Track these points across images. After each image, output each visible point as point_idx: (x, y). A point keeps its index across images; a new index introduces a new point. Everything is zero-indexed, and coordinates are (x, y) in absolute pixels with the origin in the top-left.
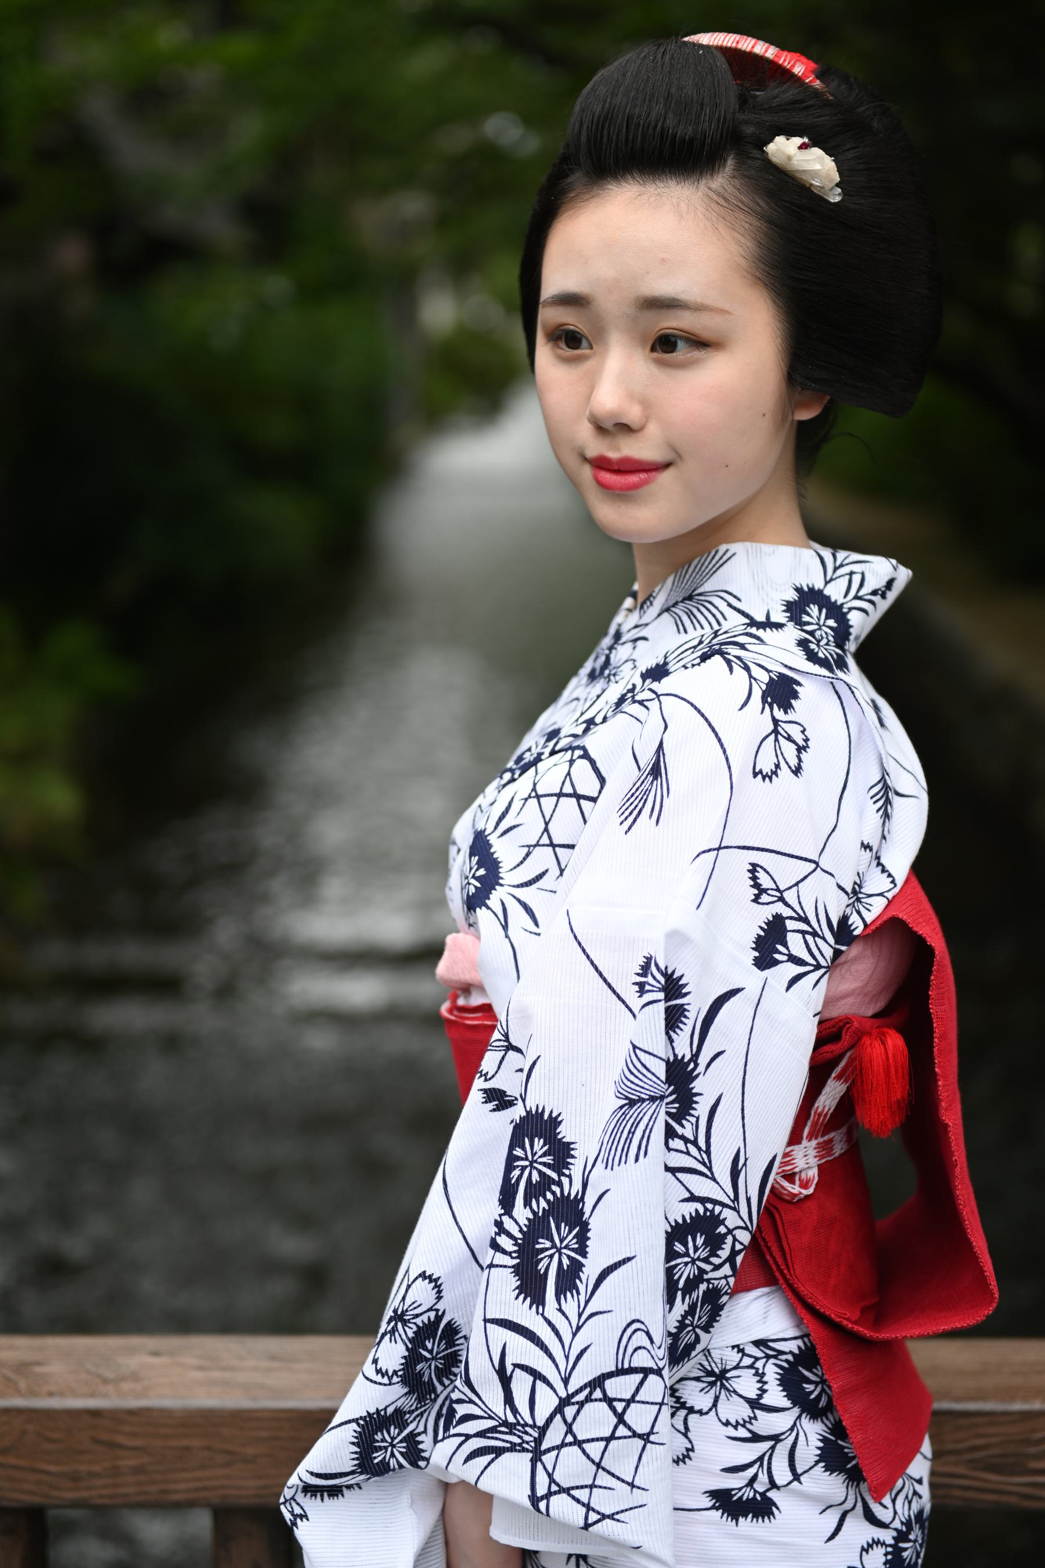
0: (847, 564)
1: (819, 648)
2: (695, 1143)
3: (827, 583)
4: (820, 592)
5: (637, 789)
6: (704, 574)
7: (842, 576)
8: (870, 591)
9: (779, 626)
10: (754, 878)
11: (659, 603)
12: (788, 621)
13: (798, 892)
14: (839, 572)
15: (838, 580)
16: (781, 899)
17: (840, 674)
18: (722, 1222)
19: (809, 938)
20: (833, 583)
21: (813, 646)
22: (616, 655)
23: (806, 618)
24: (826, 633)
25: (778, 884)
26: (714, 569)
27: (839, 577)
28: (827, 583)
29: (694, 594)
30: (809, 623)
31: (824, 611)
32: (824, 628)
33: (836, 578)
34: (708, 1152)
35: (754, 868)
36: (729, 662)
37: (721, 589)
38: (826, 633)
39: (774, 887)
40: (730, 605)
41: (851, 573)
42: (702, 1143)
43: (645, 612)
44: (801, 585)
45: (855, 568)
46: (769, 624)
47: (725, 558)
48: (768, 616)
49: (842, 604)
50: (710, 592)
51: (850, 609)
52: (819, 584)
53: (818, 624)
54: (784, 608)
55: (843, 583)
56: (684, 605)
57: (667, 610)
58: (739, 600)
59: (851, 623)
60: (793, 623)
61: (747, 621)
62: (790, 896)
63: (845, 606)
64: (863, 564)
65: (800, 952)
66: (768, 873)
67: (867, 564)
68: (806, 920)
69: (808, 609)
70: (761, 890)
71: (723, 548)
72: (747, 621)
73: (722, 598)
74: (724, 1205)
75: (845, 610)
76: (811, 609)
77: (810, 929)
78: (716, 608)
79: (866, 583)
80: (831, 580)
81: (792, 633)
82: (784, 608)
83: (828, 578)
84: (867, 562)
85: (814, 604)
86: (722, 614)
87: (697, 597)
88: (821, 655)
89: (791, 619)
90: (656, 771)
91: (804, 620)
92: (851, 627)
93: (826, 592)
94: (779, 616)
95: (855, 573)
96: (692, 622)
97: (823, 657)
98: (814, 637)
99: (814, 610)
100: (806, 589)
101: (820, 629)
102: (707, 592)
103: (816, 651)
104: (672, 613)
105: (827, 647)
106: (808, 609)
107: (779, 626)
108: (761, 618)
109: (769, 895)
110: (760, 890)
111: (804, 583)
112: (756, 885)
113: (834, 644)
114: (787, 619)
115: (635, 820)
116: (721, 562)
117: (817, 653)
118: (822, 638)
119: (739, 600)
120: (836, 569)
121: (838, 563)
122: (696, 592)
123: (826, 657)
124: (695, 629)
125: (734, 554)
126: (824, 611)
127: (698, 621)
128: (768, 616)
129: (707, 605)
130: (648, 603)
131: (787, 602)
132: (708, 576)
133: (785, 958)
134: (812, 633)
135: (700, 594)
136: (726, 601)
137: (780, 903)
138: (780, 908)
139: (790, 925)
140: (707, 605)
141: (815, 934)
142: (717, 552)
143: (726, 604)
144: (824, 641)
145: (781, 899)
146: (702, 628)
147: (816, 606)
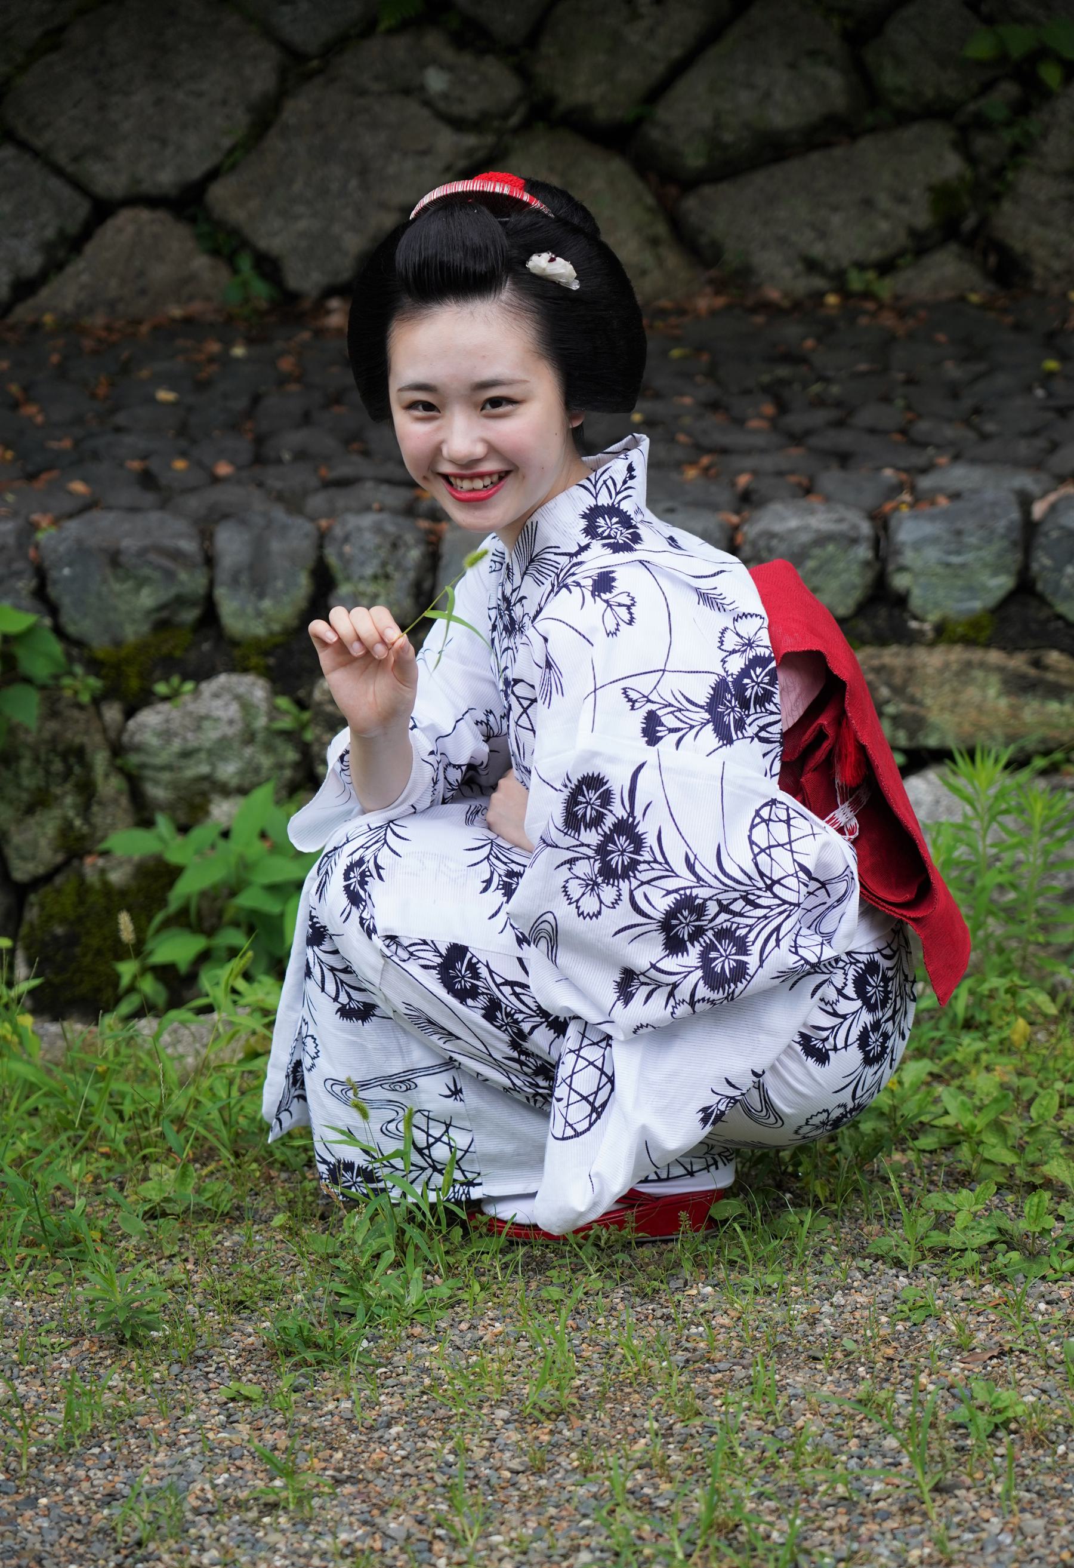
2: (656, 861)
9: (587, 547)
10: (627, 696)
16: (649, 701)
34: (667, 863)
42: (660, 859)
46: (583, 549)
70: (633, 702)
90: (549, 665)
94: (584, 541)
107: (587, 547)
110: (633, 702)
112: (630, 700)
138: (650, 707)
139: (659, 713)
141: (680, 710)
145: (649, 701)
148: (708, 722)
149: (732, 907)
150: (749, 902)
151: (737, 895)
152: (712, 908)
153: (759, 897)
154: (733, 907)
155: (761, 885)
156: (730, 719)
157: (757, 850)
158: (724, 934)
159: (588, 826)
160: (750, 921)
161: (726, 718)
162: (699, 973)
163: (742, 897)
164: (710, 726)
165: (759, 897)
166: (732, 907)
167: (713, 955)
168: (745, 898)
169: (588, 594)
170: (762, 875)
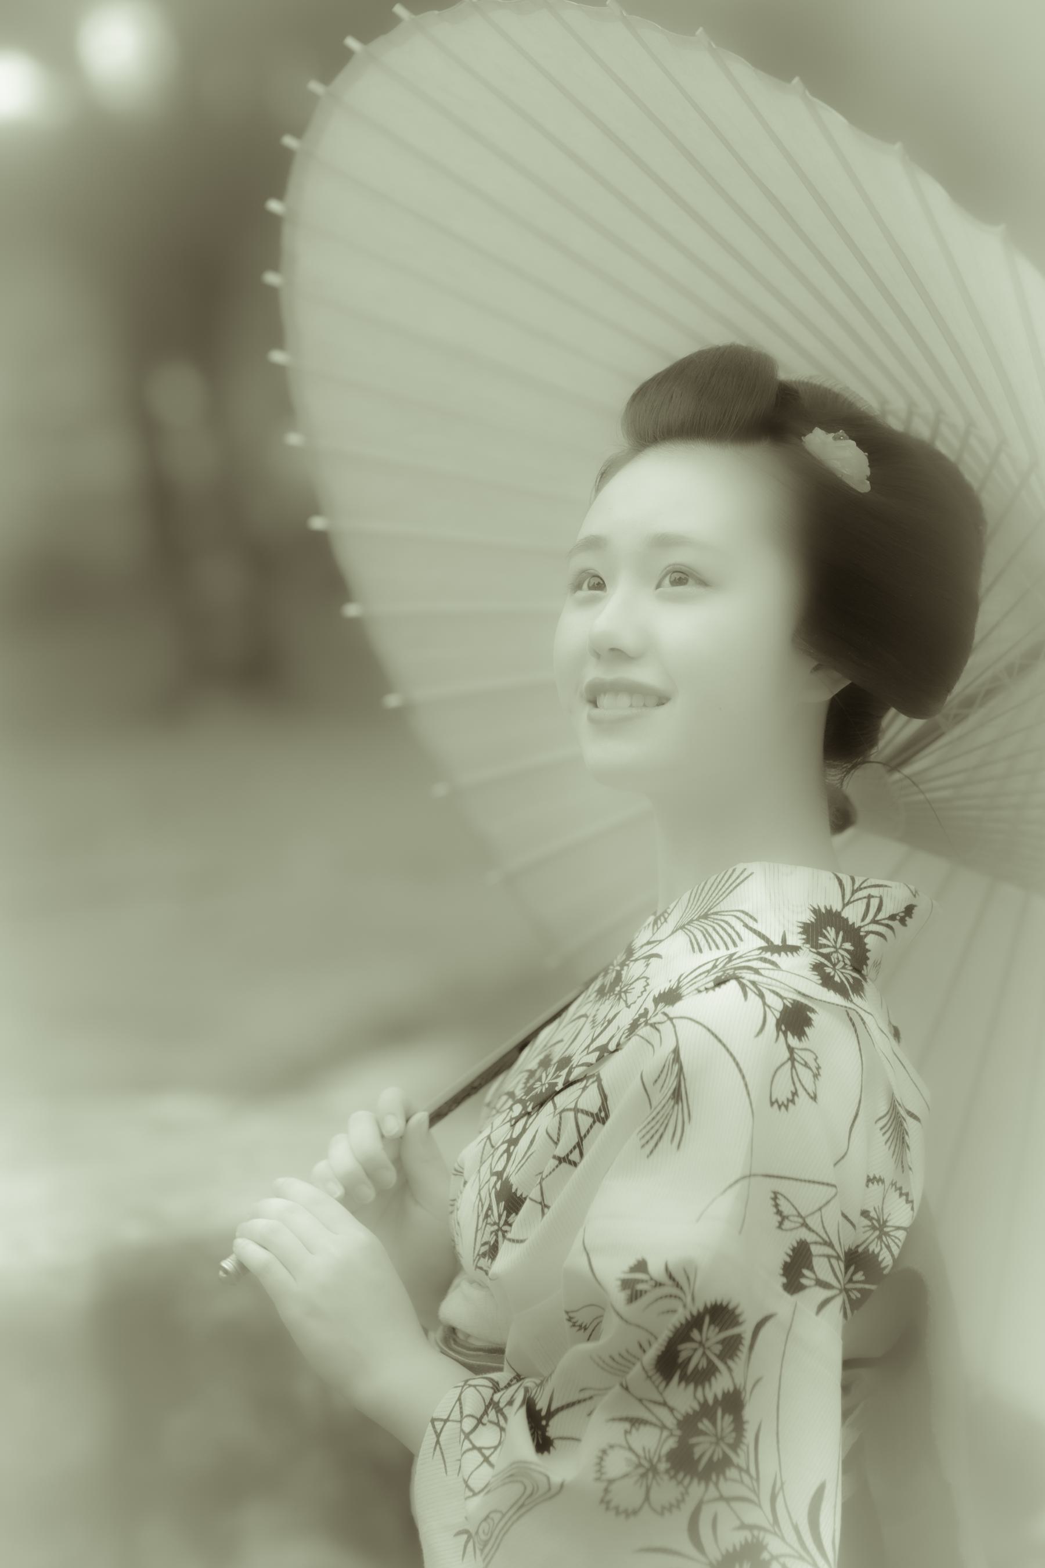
0: (865, 888)
1: (835, 971)
3: (845, 905)
4: (838, 915)
5: (658, 1113)
6: (721, 893)
7: (860, 899)
8: (887, 916)
9: (794, 949)
10: (776, 1205)
11: (673, 921)
12: (804, 943)
13: (821, 1217)
14: (858, 895)
15: (856, 903)
16: (805, 1225)
17: (856, 999)
20: (851, 905)
21: (828, 970)
22: (628, 972)
23: (823, 941)
24: (842, 956)
25: (800, 1211)
26: (731, 888)
27: (858, 900)
28: (845, 905)
29: (709, 913)
30: (825, 946)
31: (841, 934)
32: (840, 951)
33: (854, 901)
36: (743, 987)
37: (737, 909)
38: (842, 956)
39: (795, 1213)
40: (746, 926)
41: (869, 897)
43: (658, 929)
44: (818, 906)
45: (874, 892)
46: (786, 948)
47: (742, 878)
48: (784, 940)
49: (860, 927)
50: (727, 911)
51: (868, 933)
52: (837, 906)
53: (835, 947)
54: (800, 930)
55: (861, 906)
56: (699, 923)
57: (682, 927)
58: (756, 920)
59: (867, 947)
60: (808, 946)
61: (763, 944)
62: (813, 1222)
63: (862, 929)
64: (881, 889)
65: (826, 1275)
66: (788, 1200)
67: (886, 889)
69: (824, 931)
70: (783, 1217)
71: (740, 867)
72: (763, 944)
73: (738, 918)
75: (862, 934)
76: (828, 932)
77: (834, 1254)
78: (733, 928)
79: (884, 908)
80: (849, 903)
81: (807, 958)
82: (800, 930)
83: (846, 901)
84: (886, 886)
85: (831, 927)
86: (738, 934)
87: (712, 916)
88: (837, 979)
89: (807, 941)
91: (820, 942)
92: (869, 951)
93: (844, 914)
94: (795, 939)
95: (873, 897)
96: (707, 941)
97: (839, 981)
98: (830, 960)
99: (831, 932)
100: (823, 911)
101: (836, 952)
102: (723, 911)
103: (832, 974)
104: (686, 931)
105: (843, 971)
106: (824, 931)
107: (794, 949)
108: (777, 941)
109: (791, 1221)
110: (783, 1217)
111: (822, 904)
112: (779, 1212)
113: (851, 968)
114: (804, 941)
115: (656, 1145)
116: (738, 881)
117: (834, 976)
118: (839, 961)
119: (756, 920)
120: (854, 892)
121: (856, 886)
122: (712, 911)
123: (842, 981)
124: (710, 949)
125: (752, 874)
126: (841, 934)
127: (714, 941)
128: (784, 940)
129: (723, 924)
130: (662, 919)
131: (804, 923)
132: (724, 895)
134: (827, 957)
135: (716, 913)
136: (742, 921)
140: (723, 924)
142: (734, 870)
143: (742, 924)
144: (841, 964)
145: (805, 1225)
146: (718, 947)
147: (833, 929)
169: (772, 1022)
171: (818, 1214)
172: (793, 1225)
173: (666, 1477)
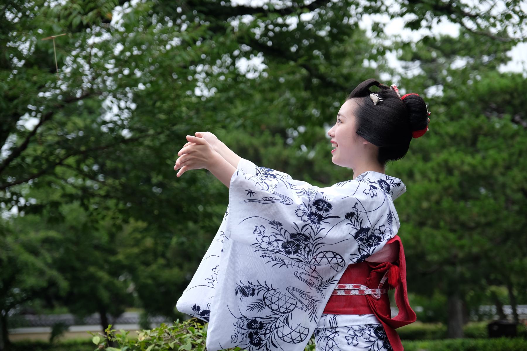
10: (355, 205)
16: (357, 212)
18: (310, 240)
19: (356, 220)
35: (357, 203)
62: (359, 213)
68: (358, 218)
70: (355, 207)
74: (312, 239)
110: (355, 207)
112: (355, 206)
133: (350, 219)
137: (356, 212)
138: (356, 213)
139: (355, 216)
141: (357, 220)
145: (357, 212)
148: (358, 230)
149: (307, 247)
150: (308, 252)
151: (311, 248)
152: (306, 243)
153: (310, 255)
154: (307, 248)
155: (314, 255)
156: (361, 236)
157: (325, 253)
158: (298, 247)
159: (317, 207)
160: (303, 254)
161: (360, 235)
162: (286, 241)
163: (310, 250)
164: (357, 231)
165: (310, 255)
166: (307, 247)
167: (291, 244)
168: (310, 251)
170: (317, 255)
171: (360, 212)
172: (355, 210)
173: (307, 216)
